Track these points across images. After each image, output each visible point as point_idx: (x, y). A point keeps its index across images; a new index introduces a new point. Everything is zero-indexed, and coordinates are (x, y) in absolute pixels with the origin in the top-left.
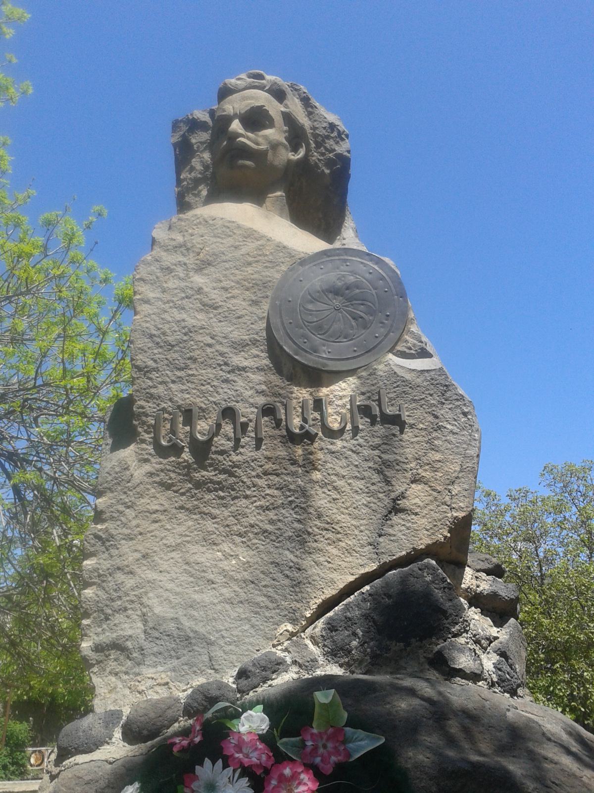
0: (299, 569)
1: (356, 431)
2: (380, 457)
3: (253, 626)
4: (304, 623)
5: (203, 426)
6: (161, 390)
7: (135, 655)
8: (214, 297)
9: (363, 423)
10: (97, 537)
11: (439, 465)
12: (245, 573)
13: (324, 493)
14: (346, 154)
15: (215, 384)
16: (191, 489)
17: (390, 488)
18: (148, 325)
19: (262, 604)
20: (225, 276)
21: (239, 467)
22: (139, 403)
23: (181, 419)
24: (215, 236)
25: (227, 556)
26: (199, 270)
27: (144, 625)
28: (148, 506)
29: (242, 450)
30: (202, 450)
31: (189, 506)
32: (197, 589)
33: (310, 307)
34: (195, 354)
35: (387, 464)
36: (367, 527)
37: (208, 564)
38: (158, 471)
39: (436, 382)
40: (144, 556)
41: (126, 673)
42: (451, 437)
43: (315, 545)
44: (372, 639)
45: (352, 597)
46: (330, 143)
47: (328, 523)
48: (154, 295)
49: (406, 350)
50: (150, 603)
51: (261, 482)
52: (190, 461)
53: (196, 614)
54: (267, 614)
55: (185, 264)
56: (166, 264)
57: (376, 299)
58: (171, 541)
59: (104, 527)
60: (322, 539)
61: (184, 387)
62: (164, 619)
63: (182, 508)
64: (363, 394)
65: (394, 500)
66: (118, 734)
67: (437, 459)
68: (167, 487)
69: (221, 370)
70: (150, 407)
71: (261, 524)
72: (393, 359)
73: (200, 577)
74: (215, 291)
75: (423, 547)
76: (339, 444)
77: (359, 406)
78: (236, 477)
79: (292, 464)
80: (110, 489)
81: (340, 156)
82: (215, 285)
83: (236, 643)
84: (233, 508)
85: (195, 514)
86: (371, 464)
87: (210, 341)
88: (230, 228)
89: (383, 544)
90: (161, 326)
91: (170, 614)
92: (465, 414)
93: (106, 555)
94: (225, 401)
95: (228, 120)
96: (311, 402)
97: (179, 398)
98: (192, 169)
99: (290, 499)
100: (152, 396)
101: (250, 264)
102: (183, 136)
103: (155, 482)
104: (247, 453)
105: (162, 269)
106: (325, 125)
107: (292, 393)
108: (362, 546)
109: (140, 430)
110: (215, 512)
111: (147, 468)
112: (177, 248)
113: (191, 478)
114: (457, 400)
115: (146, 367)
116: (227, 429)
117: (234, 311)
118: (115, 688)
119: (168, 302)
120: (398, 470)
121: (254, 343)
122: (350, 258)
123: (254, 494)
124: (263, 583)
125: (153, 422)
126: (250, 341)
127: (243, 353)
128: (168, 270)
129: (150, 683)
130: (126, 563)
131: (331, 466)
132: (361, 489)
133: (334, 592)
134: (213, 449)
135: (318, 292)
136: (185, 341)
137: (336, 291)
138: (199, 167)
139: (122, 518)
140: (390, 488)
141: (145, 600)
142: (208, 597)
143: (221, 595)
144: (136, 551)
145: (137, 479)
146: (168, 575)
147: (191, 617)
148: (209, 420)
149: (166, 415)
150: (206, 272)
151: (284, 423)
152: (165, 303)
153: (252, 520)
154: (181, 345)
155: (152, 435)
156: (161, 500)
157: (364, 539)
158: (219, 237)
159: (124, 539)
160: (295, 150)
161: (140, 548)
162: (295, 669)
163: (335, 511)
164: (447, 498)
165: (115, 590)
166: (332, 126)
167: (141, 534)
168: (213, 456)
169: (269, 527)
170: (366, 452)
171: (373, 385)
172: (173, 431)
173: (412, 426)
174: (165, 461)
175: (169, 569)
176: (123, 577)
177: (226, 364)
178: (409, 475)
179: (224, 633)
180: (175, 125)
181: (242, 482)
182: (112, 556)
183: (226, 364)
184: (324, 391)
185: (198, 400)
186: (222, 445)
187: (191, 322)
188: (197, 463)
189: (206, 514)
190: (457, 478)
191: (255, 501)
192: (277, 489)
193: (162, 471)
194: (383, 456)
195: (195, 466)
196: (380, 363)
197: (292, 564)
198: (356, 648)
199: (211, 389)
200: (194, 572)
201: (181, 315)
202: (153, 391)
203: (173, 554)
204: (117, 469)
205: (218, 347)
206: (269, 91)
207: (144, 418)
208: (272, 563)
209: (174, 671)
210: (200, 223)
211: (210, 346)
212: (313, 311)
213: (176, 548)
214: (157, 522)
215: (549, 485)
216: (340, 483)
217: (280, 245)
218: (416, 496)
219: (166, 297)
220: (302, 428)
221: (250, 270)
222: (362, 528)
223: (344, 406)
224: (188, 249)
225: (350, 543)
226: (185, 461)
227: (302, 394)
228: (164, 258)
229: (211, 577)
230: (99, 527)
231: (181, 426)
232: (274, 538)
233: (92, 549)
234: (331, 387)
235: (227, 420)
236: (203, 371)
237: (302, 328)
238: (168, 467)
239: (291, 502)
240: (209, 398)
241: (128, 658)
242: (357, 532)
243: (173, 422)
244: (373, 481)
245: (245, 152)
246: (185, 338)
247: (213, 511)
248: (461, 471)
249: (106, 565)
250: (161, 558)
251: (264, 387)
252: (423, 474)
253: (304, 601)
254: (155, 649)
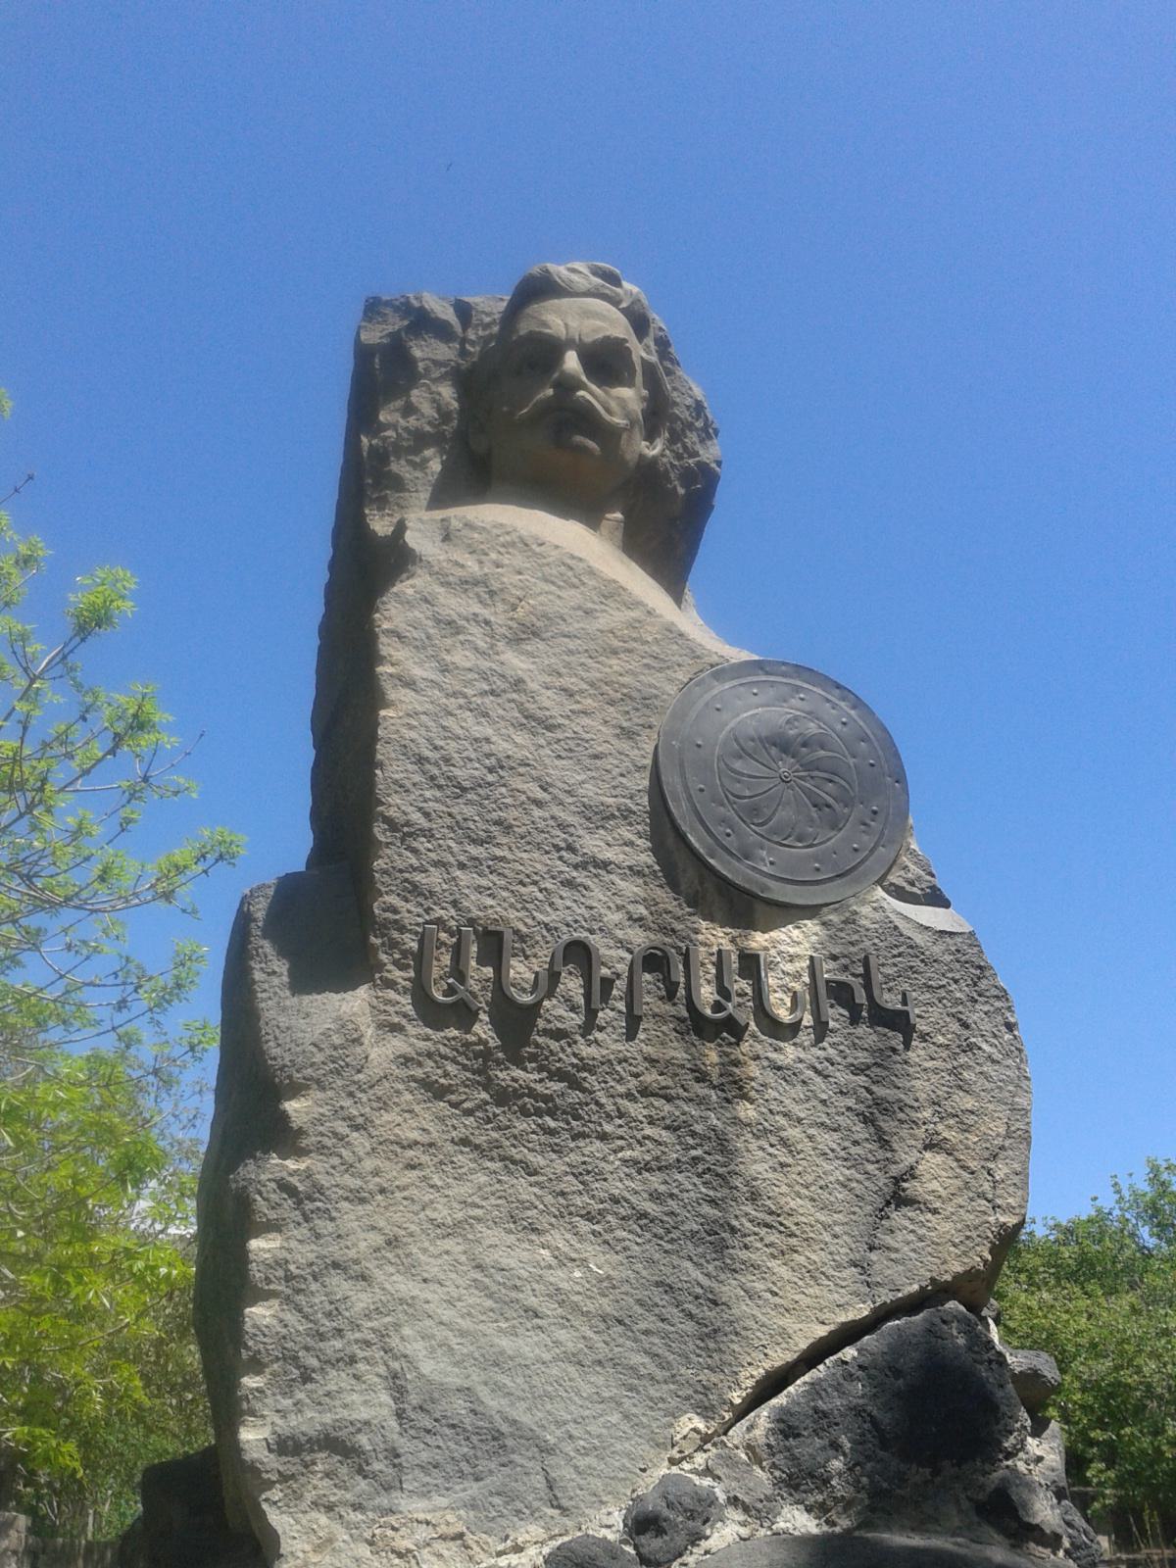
0: (715, 1303)
1: (821, 1030)
2: (868, 1090)
3: (626, 1417)
4: (728, 1416)
5: (520, 971)
6: (434, 879)
7: (377, 1466)
8: (547, 703)
9: (835, 1015)
10: (285, 1187)
11: (971, 1119)
12: (604, 1301)
13: (761, 1148)
14: (713, 465)
15: (548, 885)
16: (487, 1103)
17: (889, 1155)
18: (413, 734)
19: (643, 1371)
20: (568, 665)
21: (591, 1070)
22: (387, 898)
23: (474, 948)
24: (546, 580)
25: (563, 1261)
26: (515, 641)
27: (395, 1399)
28: (397, 1130)
29: (599, 1035)
30: (516, 1022)
31: (480, 1140)
32: (504, 1325)
33: (738, 765)
34: (510, 815)
35: (882, 1106)
36: (846, 1228)
37: (525, 1274)
38: (419, 1054)
39: (963, 959)
40: (389, 1243)
41: (357, 1507)
42: (988, 1068)
43: (744, 1255)
44: (869, 1458)
45: (821, 1367)
47: (771, 1213)
48: (425, 674)
49: (905, 884)
50: (409, 1349)
51: (636, 1109)
52: (492, 1044)
53: (507, 1381)
54: (652, 1392)
55: (487, 623)
56: (445, 612)
57: (855, 777)
58: (442, 1213)
59: (302, 1166)
60: (759, 1245)
61: (484, 882)
62: (444, 1389)
63: (465, 1142)
64: (834, 958)
65: (897, 1180)
67: (969, 1106)
68: (438, 1092)
69: (561, 858)
70: (409, 912)
71: (633, 1199)
73: (508, 1300)
74: (549, 693)
75: (948, 1277)
76: (789, 1053)
77: (828, 982)
78: (584, 1090)
79: (698, 1080)
80: (318, 1082)
81: (703, 467)
82: (548, 679)
83: (596, 1450)
84: (574, 1158)
85: (492, 1159)
86: (851, 1102)
87: (540, 795)
89: (877, 1267)
90: (441, 743)
91: (454, 1380)
92: (1010, 1027)
93: (304, 1231)
94: (568, 925)
96: (734, 957)
97: (472, 902)
98: (409, 410)
99: (694, 1153)
100: (414, 890)
101: (615, 652)
102: (395, 336)
103: (413, 1079)
104: (609, 1043)
105: (438, 621)
106: (689, 401)
107: (697, 932)
108: (839, 1267)
109: (384, 957)
110: (537, 1160)
111: (397, 1044)
112: (467, 584)
113: (489, 1079)
114: (997, 997)
115: (408, 824)
116: (571, 985)
117: (587, 741)
118: (330, 1541)
119: (454, 695)
120: (901, 1122)
121: (626, 814)
122: (805, 685)
123: (620, 1132)
124: (643, 1326)
125: (415, 945)
126: (619, 809)
127: (602, 832)
128: (452, 627)
129: (423, 1533)
130: (352, 1253)
131: (774, 1094)
132: (833, 1150)
133: (790, 1357)
134: (541, 1023)
135: (753, 740)
136: (490, 784)
137: (783, 745)
138: (427, 409)
139: (344, 1152)
140: (889, 1155)
141: (394, 1342)
142: (527, 1345)
143: (557, 1343)
144: (374, 1228)
145: (374, 1070)
146: (440, 1290)
147: (498, 1389)
148: (534, 960)
149: (443, 936)
150: (529, 648)
151: (681, 992)
152: (448, 696)
153: (616, 1188)
154: (480, 791)
155: (412, 974)
156: (417, 1120)
157: (843, 1253)
158: (553, 583)
159: (346, 1199)
161: (382, 1224)
162: (737, 1515)
163: (784, 1189)
164: (987, 1186)
165: (328, 1315)
167: (382, 1191)
168: (540, 1040)
169: (649, 1207)
170: (843, 1077)
171: (852, 944)
172: (459, 973)
173: (924, 1037)
174: (437, 1035)
175: (442, 1276)
176: (346, 1285)
177: (571, 848)
178: (920, 1132)
179: (571, 1427)
180: (373, 309)
181: (597, 1103)
182: (318, 1236)
183: (571, 848)
184: (758, 940)
185: (512, 914)
186: (560, 1018)
187: (501, 747)
189: (514, 1162)
190: (1002, 1148)
191: (622, 1149)
192: (667, 1128)
193: (429, 1055)
194: (874, 1088)
195: (500, 1055)
196: (864, 902)
197: (701, 1291)
198: (840, 1475)
199: (540, 896)
200: (494, 1288)
201: (480, 728)
202: (418, 877)
203: (448, 1244)
204: (337, 1040)
205: (557, 811)
206: (624, 311)
207: (395, 935)
208: (658, 1284)
209: (474, 1507)
210: (513, 544)
211: (539, 803)
212: (743, 775)
214: (413, 1167)
216: (793, 1133)
217: (673, 629)
218: (934, 1175)
219: (448, 681)
220: (718, 1007)
222: (837, 1229)
223: (797, 976)
224: (492, 593)
225: (814, 1257)
226: (481, 1041)
227: (715, 937)
228: (442, 600)
229: (533, 1302)
230: (291, 1164)
231: (473, 963)
232: (661, 1231)
233: (272, 1215)
234: (774, 934)
235: (570, 967)
236: (525, 855)
237: (723, 805)
238: (443, 1050)
239: (696, 1160)
240: (535, 914)
241: (360, 1471)
242: (827, 1238)
243: (458, 952)
244: (856, 1137)
246: (490, 778)
247: (531, 1157)
248: (1008, 1136)
249: (304, 1253)
250: (425, 1251)
251: (642, 910)
252: (946, 1134)
254: (425, 1456)
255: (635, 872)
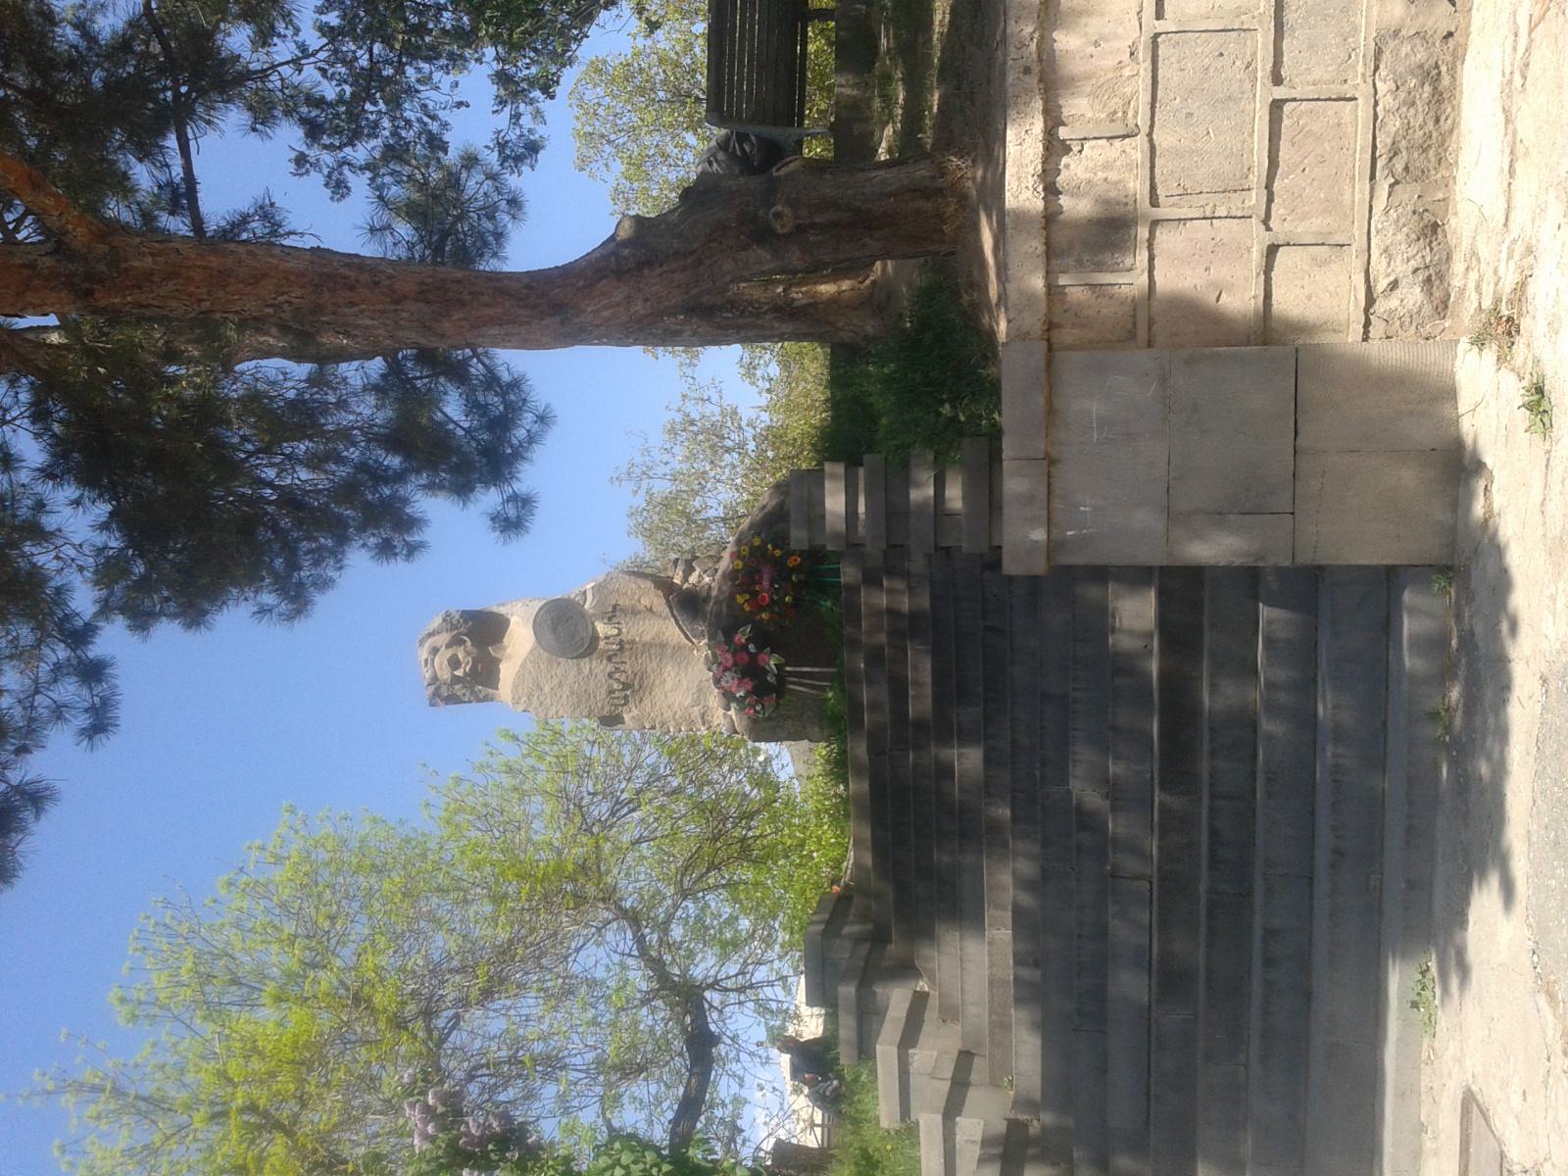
5: (615, 686)
6: (599, 705)
9: (615, 620)
26: (542, 690)
30: (626, 686)
35: (633, 612)
46: (455, 622)
66: (729, 713)
70: (607, 709)
72: (586, 607)
88: (520, 675)
95: (456, 680)
98: (464, 695)
104: (627, 667)
111: (633, 709)
128: (541, 703)
137: (554, 630)
142: (685, 682)
160: (465, 641)
166: (444, 620)
170: (628, 619)
180: (431, 705)
187: (568, 693)
188: (632, 688)
213: (666, 696)
215: (607, 165)
218: (645, 601)
221: (542, 666)
227: (602, 644)
245: (474, 668)
253: (685, 645)
255: (591, 662)
